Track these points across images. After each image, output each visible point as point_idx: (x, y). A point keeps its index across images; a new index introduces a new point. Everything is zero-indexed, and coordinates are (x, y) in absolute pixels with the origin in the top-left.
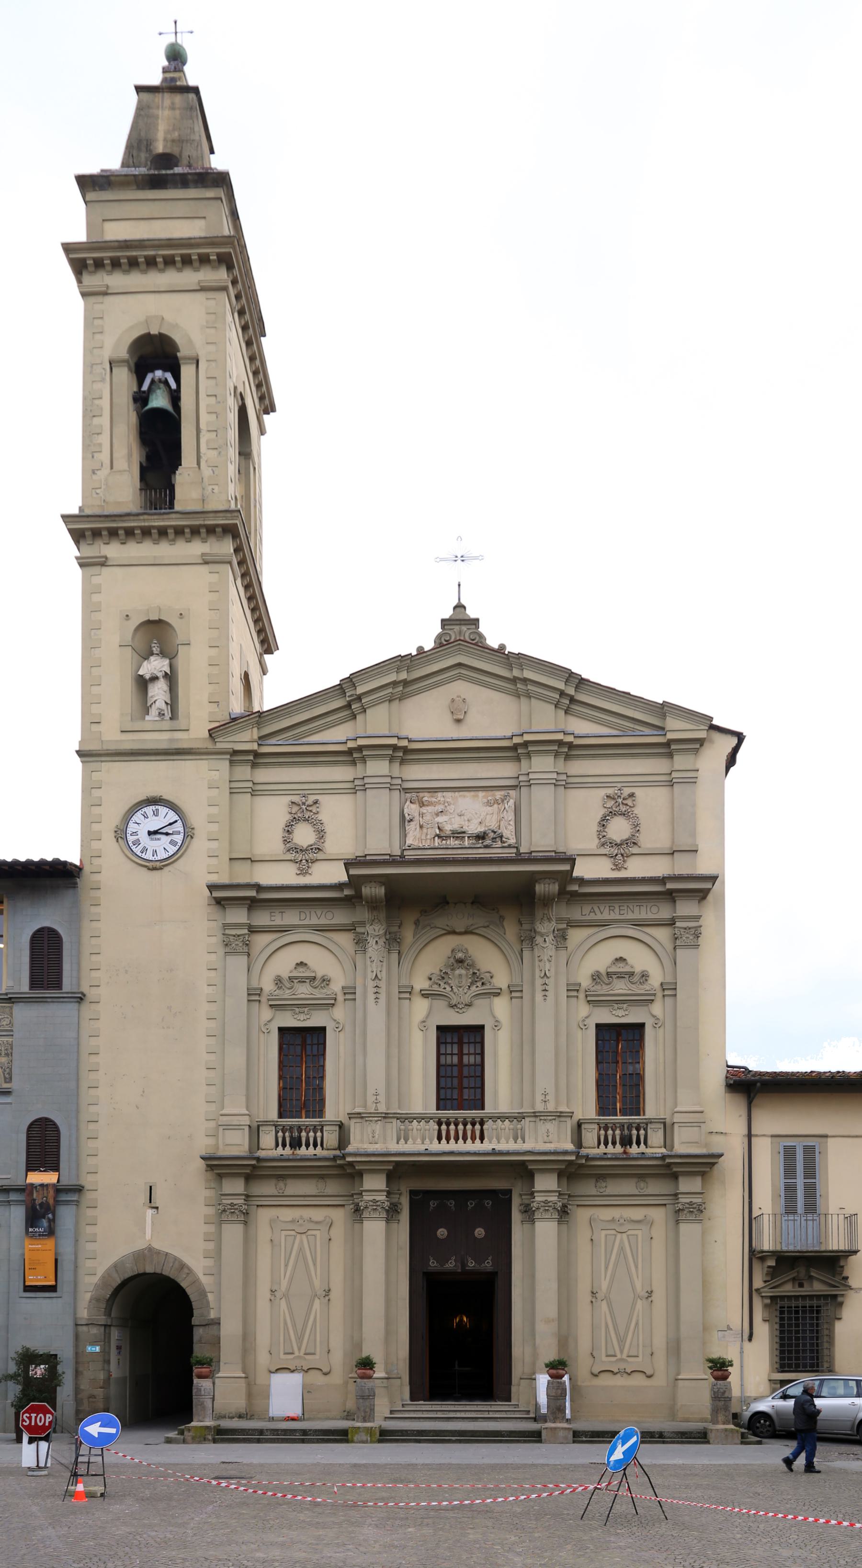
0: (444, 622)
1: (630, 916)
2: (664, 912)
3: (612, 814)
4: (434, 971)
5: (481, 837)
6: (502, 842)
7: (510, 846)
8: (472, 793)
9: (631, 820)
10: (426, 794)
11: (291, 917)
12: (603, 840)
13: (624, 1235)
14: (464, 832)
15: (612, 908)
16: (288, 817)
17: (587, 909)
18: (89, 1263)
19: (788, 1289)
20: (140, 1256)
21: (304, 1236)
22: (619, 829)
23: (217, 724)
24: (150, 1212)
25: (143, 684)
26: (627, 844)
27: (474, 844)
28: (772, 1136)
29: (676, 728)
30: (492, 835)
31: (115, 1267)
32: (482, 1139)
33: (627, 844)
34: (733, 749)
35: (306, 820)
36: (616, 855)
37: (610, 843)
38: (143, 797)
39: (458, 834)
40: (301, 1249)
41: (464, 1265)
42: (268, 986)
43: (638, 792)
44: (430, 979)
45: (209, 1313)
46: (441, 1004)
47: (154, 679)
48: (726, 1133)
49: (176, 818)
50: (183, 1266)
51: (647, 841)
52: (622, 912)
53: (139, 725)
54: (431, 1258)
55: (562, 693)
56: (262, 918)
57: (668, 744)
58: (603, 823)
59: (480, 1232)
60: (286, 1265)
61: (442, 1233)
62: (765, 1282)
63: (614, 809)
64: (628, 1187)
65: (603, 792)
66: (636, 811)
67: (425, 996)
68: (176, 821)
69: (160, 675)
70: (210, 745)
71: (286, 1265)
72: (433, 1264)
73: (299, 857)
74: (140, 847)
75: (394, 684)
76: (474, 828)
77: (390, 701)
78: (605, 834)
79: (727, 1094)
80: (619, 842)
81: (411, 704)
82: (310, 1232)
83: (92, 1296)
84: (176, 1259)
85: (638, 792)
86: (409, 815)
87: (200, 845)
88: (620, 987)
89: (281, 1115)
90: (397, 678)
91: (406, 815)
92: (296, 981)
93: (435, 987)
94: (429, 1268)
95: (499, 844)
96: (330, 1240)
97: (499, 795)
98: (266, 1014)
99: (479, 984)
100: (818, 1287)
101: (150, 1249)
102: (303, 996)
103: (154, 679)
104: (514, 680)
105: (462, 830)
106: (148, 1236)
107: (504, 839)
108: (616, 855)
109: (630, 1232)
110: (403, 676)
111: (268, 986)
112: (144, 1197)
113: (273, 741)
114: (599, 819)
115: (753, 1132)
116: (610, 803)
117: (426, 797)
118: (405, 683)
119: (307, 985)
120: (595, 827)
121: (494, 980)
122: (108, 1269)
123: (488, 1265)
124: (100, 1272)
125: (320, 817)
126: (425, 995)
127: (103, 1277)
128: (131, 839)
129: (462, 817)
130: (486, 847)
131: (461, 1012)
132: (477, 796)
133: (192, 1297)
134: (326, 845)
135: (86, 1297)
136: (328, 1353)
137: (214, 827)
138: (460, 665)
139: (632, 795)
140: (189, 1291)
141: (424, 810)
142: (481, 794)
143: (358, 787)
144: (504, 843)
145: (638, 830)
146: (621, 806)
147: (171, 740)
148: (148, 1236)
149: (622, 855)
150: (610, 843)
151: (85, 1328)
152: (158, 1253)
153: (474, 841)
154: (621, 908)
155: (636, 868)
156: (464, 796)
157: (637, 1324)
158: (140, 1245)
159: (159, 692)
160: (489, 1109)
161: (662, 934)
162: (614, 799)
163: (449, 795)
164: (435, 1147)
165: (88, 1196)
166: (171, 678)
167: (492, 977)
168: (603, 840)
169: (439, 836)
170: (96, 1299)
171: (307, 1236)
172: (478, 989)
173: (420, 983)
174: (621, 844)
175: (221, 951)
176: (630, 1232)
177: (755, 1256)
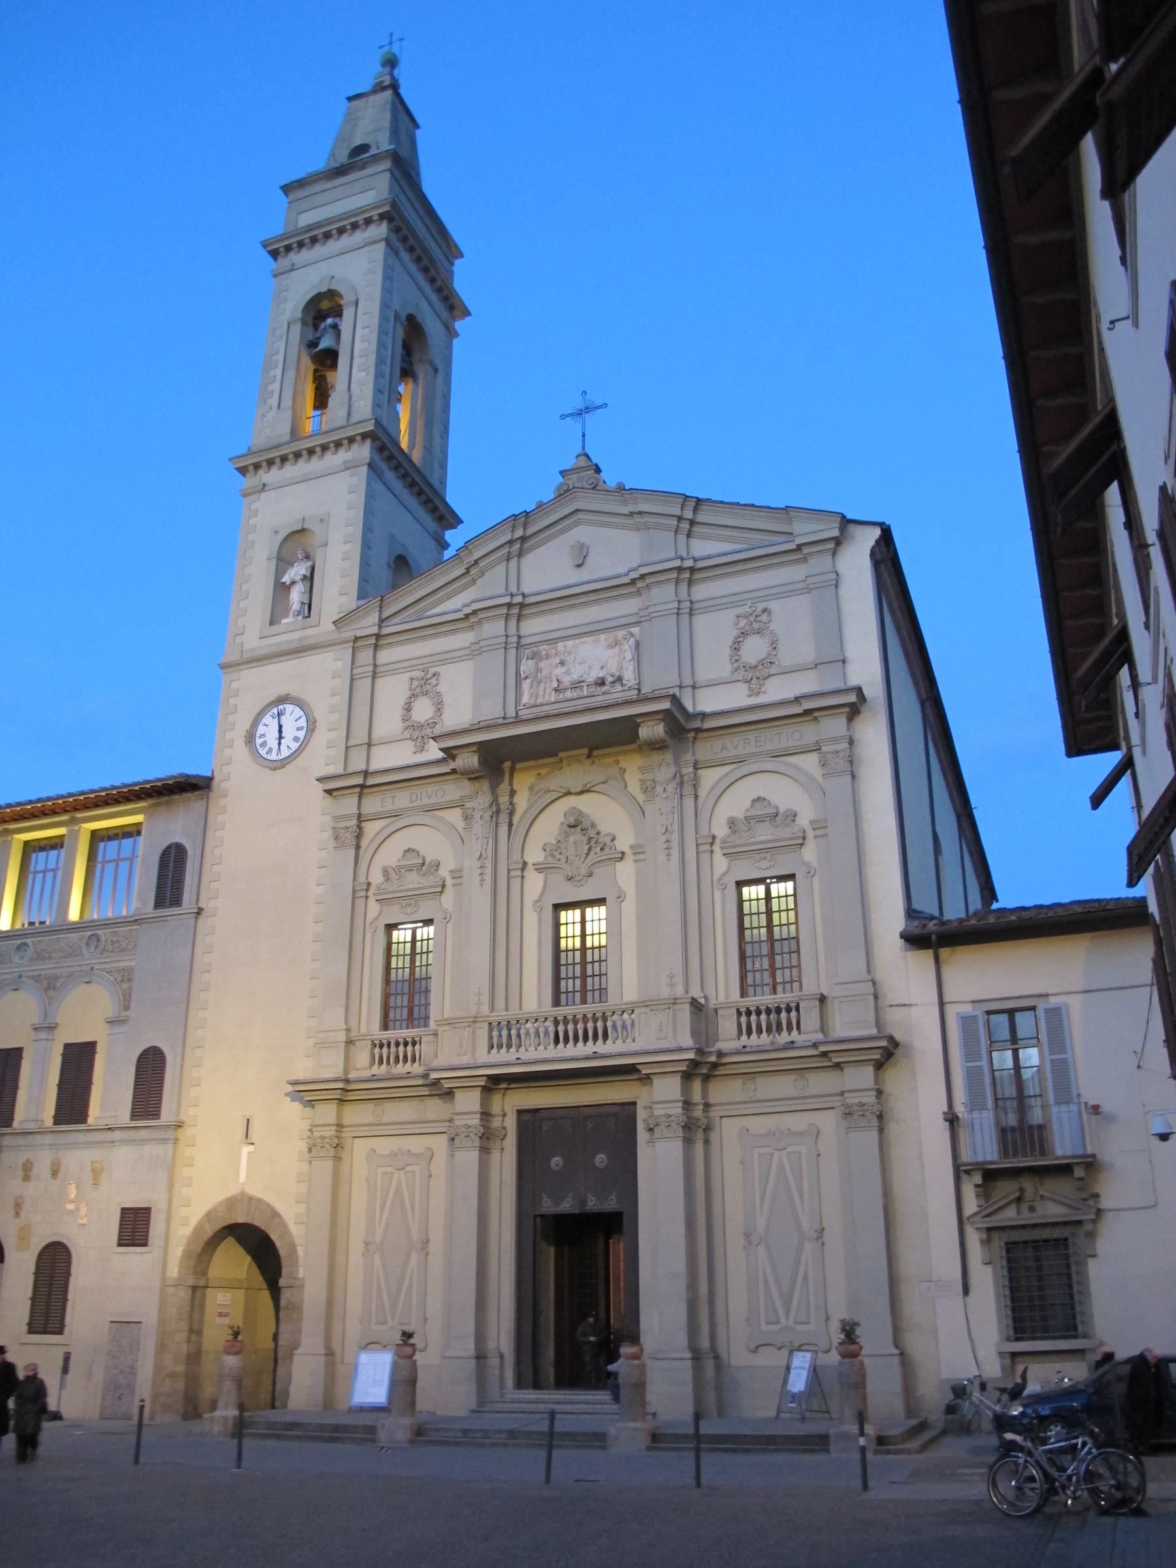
0: (563, 473)
1: (769, 746)
2: (808, 733)
3: (744, 634)
4: (548, 841)
5: (601, 683)
6: (622, 685)
7: (630, 689)
8: (593, 638)
9: (766, 638)
10: (546, 647)
11: (402, 799)
12: (735, 665)
13: (784, 1152)
14: (583, 681)
15: (747, 741)
16: (409, 694)
17: (718, 744)
18: (183, 1212)
19: (1010, 1215)
20: (231, 1203)
21: (402, 1173)
22: (755, 649)
23: (343, 614)
24: (246, 1149)
25: (282, 589)
26: (763, 664)
27: (594, 692)
28: (973, 1002)
29: (805, 530)
30: (610, 679)
31: (208, 1214)
32: (606, 1036)
33: (763, 664)
34: (876, 541)
35: (426, 693)
36: (751, 679)
37: (744, 667)
38: (272, 698)
39: (577, 685)
40: (398, 1191)
41: (583, 1202)
42: (376, 878)
43: (773, 605)
44: (545, 850)
45: (297, 1271)
46: (557, 878)
47: (293, 583)
48: (910, 1005)
49: (301, 713)
50: (275, 1214)
51: (787, 656)
52: (759, 744)
53: (275, 629)
54: (544, 1196)
55: (680, 519)
56: (373, 804)
57: (799, 548)
58: (736, 647)
59: (601, 1159)
60: (382, 1211)
61: (556, 1162)
62: (979, 1206)
63: (746, 628)
64: (784, 1086)
65: (731, 613)
66: (772, 626)
67: (539, 870)
68: (301, 717)
69: (298, 578)
70: (336, 636)
71: (382, 1211)
72: (548, 1206)
73: (416, 734)
74: (266, 749)
75: (511, 542)
76: (595, 674)
77: (508, 560)
78: (737, 658)
79: (909, 954)
80: (754, 663)
81: (529, 560)
82: (409, 1168)
83: (184, 1251)
84: (268, 1205)
85: (773, 605)
86: (524, 672)
87: (322, 736)
88: (765, 833)
89: (385, 1027)
90: (512, 535)
91: (522, 673)
92: (403, 870)
93: (550, 860)
94: (543, 1209)
95: (619, 688)
96: (430, 1176)
97: (621, 634)
98: (373, 908)
99: (598, 850)
100: (1052, 1211)
101: (243, 1194)
102: (411, 886)
103: (293, 583)
104: (631, 514)
105: (582, 679)
106: (243, 1177)
107: (624, 682)
108: (751, 679)
109: (790, 1149)
110: (519, 533)
111: (376, 878)
112: (241, 1133)
113: (397, 620)
114: (730, 643)
115: (947, 999)
116: (743, 622)
117: (544, 649)
118: (523, 539)
119: (414, 873)
120: (727, 652)
121: (616, 842)
122: (201, 1220)
123: (611, 1204)
124: (193, 1223)
125: (439, 689)
126: (539, 869)
127: (195, 1229)
128: (259, 741)
129: (583, 665)
130: (605, 693)
131: (579, 884)
132: (598, 640)
133: (283, 1252)
134: (443, 717)
135: (177, 1251)
136: (425, 1323)
137: (335, 717)
138: (577, 511)
139: (765, 610)
140: (278, 1244)
141: (542, 664)
142: (602, 637)
143: (475, 651)
144: (625, 685)
145: (775, 648)
146: (754, 623)
147: (301, 639)
148: (243, 1177)
149: (758, 678)
150: (744, 667)
151: (171, 1290)
152: (251, 1198)
153: (594, 689)
154: (758, 739)
155: (778, 690)
156: (585, 643)
157: (806, 1277)
158: (232, 1191)
159: (296, 596)
160: (613, 1000)
161: (809, 762)
162: (745, 617)
163: (569, 643)
164: (552, 1052)
165: (187, 1133)
166: (310, 579)
167: (613, 840)
168: (735, 665)
169: (556, 690)
170: (187, 1254)
171: (405, 1172)
172: (597, 855)
173: (535, 855)
174: (756, 667)
175: (333, 844)
176: (790, 1149)
177: (960, 1171)
